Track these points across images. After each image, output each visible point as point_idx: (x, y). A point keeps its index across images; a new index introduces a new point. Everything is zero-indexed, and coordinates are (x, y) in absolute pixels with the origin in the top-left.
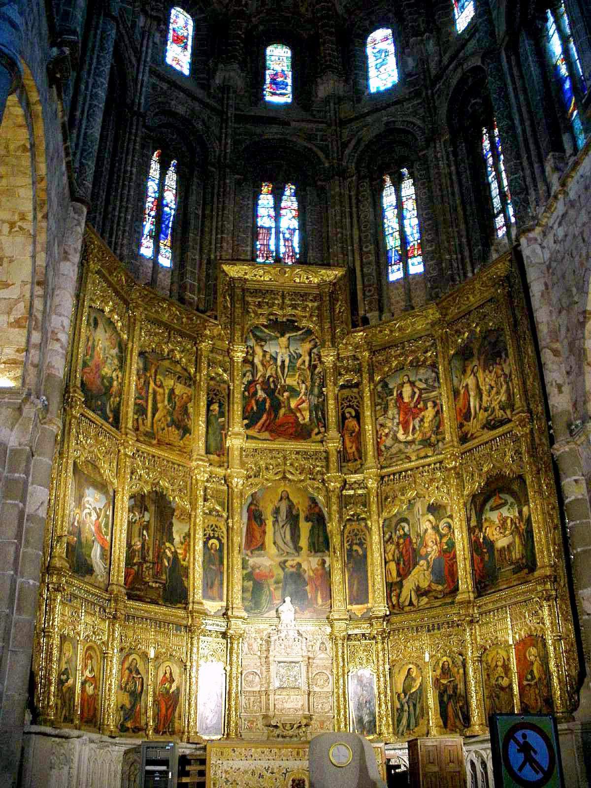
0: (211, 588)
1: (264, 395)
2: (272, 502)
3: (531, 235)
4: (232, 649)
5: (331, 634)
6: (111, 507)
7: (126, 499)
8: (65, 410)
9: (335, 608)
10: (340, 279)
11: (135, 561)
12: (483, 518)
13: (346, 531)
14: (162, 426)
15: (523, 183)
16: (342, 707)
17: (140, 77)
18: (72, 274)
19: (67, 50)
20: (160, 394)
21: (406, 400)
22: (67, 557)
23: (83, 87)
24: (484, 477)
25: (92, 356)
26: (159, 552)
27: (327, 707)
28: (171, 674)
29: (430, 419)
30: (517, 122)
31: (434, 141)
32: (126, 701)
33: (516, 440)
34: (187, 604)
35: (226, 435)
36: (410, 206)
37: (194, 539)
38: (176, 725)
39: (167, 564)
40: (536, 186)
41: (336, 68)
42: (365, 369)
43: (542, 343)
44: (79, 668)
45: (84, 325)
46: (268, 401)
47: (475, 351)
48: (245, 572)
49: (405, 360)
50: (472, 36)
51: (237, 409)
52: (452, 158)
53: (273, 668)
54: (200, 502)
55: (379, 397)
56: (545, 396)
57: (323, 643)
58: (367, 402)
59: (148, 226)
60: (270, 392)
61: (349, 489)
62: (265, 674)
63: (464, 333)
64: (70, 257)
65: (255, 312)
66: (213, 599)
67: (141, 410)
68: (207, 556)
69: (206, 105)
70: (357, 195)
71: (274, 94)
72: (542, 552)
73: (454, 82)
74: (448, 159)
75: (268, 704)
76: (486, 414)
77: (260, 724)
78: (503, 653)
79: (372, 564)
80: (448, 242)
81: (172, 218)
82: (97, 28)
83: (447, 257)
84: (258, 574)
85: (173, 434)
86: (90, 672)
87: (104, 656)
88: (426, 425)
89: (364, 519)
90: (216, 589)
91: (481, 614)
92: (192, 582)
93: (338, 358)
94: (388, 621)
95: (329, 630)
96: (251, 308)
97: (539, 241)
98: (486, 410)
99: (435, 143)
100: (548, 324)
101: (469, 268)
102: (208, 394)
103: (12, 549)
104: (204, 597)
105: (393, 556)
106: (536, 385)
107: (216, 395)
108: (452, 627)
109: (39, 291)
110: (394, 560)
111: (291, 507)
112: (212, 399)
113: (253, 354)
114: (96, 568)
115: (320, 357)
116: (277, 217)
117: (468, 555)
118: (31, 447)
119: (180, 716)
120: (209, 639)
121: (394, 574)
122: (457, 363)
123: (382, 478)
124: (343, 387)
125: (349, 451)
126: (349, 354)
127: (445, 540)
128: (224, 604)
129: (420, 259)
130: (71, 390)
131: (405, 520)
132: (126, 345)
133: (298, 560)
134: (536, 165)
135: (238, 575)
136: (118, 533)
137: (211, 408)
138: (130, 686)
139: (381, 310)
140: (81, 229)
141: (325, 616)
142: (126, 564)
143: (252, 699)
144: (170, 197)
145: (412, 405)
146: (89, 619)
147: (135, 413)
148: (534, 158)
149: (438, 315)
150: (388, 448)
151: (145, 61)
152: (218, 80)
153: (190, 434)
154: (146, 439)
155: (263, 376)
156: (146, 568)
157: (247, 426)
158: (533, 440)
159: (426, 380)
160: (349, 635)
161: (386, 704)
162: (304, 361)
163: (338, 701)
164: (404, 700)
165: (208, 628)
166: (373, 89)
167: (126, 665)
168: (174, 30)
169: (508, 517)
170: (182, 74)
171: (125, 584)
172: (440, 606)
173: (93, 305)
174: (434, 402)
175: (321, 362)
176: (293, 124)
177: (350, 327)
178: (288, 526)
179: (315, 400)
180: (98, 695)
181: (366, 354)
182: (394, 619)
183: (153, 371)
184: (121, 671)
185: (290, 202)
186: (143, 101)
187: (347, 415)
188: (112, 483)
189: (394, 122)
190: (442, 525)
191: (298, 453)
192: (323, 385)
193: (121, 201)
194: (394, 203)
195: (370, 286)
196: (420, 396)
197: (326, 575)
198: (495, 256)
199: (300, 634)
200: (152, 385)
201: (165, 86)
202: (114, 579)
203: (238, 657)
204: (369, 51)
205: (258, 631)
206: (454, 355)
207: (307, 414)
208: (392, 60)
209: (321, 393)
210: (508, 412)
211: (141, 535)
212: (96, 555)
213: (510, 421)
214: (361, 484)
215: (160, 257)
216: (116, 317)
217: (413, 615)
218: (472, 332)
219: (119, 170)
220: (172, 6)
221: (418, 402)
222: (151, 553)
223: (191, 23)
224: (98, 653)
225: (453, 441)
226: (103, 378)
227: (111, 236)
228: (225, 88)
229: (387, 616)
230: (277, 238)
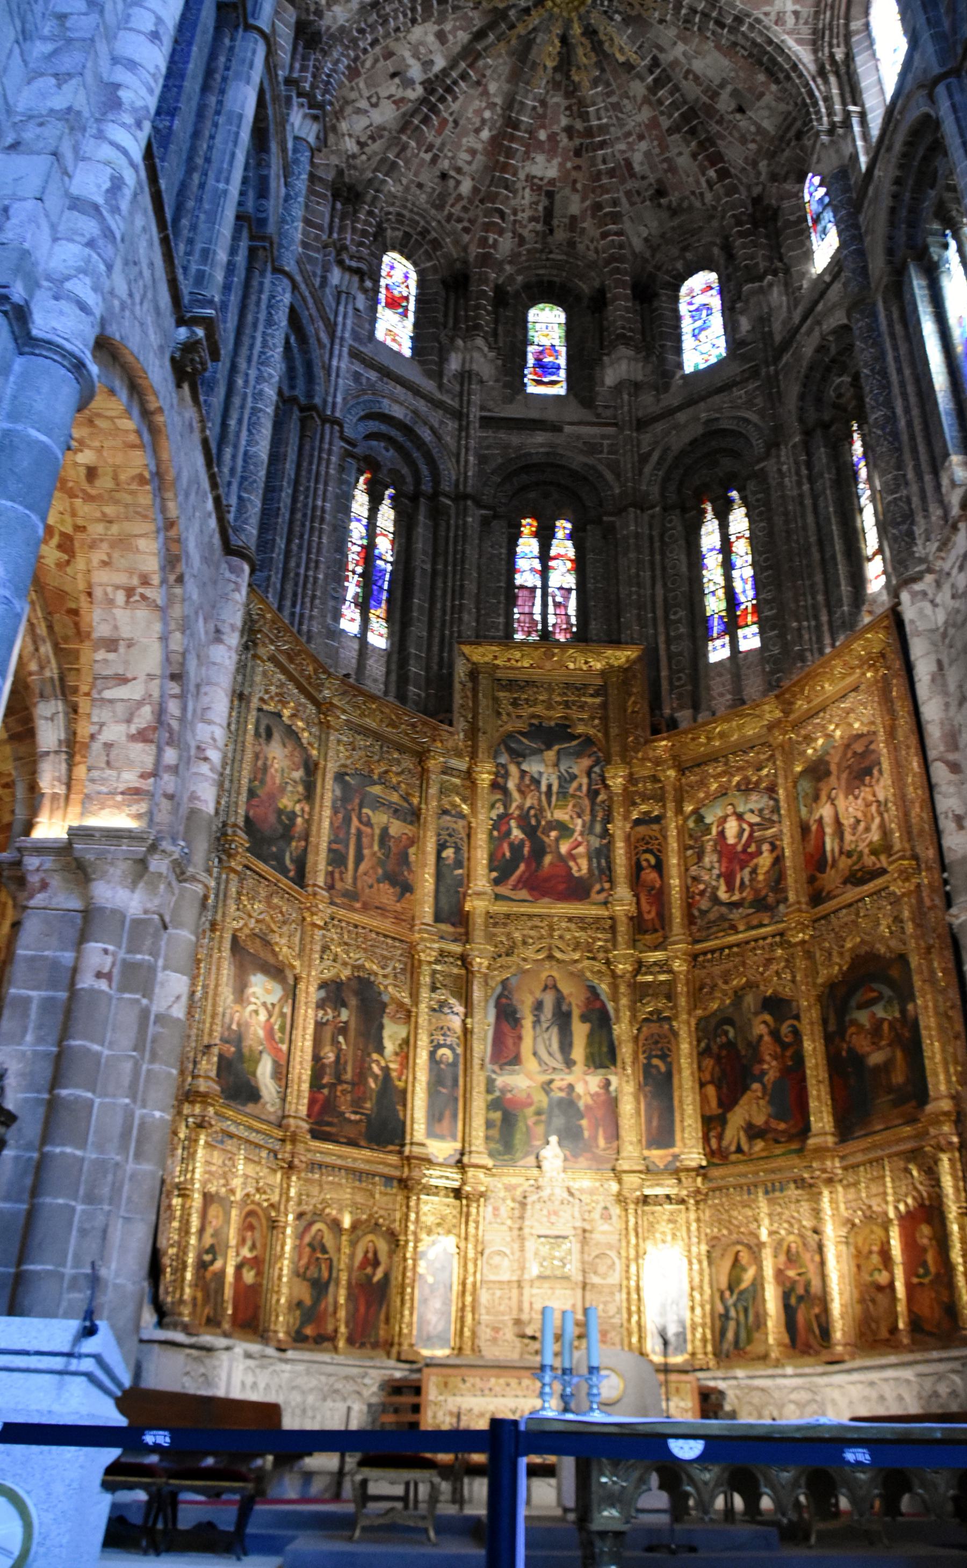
0: (440, 1120)
1: (522, 836)
2: (531, 993)
3: (917, 587)
4: (468, 1215)
5: (619, 1194)
7: (312, 989)
8: (220, 861)
9: (624, 1154)
10: (635, 662)
12: (847, 1018)
13: (642, 1037)
15: (905, 507)
16: (634, 1308)
17: (335, 363)
18: (227, 662)
19: (200, 332)
21: (731, 840)
22: (218, 1075)
23: (240, 382)
24: (847, 957)
25: (263, 782)
26: (362, 1068)
27: (612, 1309)
28: (375, 1253)
29: (765, 869)
30: (899, 410)
31: (777, 445)
32: (304, 1293)
33: (896, 901)
34: (403, 1145)
35: (465, 895)
36: (741, 549)
37: (415, 1047)
38: (382, 1333)
39: (373, 1085)
40: (925, 510)
41: (631, 338)
42: (670, 795)
43: (932, 754)
44: (233, 1242)
45: (250, 737)
46: (527, 844)
47: (833, 768)
48: (490, 1097)
49: (730, 781)
50: (835, 277)
51: (481, 856)
52: (804, 472)
53: (530, 1245)
54: (425, 994)
55: (691, 836)
56: (938, 833)
57: (606, 1208)
58: (673, 845)
59: (352, 588)
60: (531, 831)
61: (646, 974)
62: (518, 1254)
63: (816, 739)
64: (225, 637)
65: (508, 714)
66: (441, 1137)
67: (337, 859)
69: (437, 404)
70: (662, 536)
71: (539, 383)
72: (936, 1075)
73: (808, 351)
74: (798, 473)
75: (520, 1302)
76: (850, 862)
77: (509, 1333)
78: (879, 1232)
79: (681, 1087)
80: (797, 601)
81: (387, 577)
82: (261, 291)
83: (795, 624)
84: (510, 1100)
85: (386, 894)
87: (273, 1225)
88: (761, 878)
89: (668, 1019)
90: (446, 1122)
91: (845, 1169)
92: (409, 1112)
93: (631, 779)
94: (705, 1177)
95: (614, 1187)
96: (506, 706)
97: (930, 596)
98: (849, 855)
99: (779, 449)
100: (942, 723)
101: (827, 641)
102: (439, 835)
103: (128, 1066)
104: (430, 1134)
105: (712, 1074)
106: (924, 815)
108: (803, 1188)
109: (175, 689)
110: (711, 1082)
111: (560, 1000)
113: (506, 775)
115: (603, 780)
116: (544, 573)
117: (823, 1075)
118: (162, 917)
119: (387, 1321)
120: (435, 1199)
121: (714, 1103)
122: (805, 786)
123: (695, 957)
124: (637, 822)
125: (647, 917)
126: (646, 773)
127: (788, 1053)
128: (458, 1145)
129: (755, 629)
130: (230, 831)
131: (730, 1021)
132: (316, 765)
133: (570, 1079)
134: (928, 478)
135: (479, 1103)
136: (300, 1039)
137: (444, 854)
138: (313, 1272)
139: (696, 707)
140: (241, 596)
141: (609, 1166)
142: (312, 1086)
143: (498, 1293)
144: (384, 545)
145: (739, 848)
146: (251, 1170)
147: (329, 864)
148: (925, 467)
149: (778, 714)
150: (704, 913)
151: (342, 339)
152: (454, 364)
154: (345, 900)
155: (520, 807)
157: (497, 882)
158: (920, 901)
159: (761, 811)
160: (646, 1196)
161: (702, 1306)
162: (580, 786)
163: (628, 1300)
164: (730, 1302)
165: (433, 1182)
166: (688, 368)
167: (307, 1239)
168: (387, 286)
169: (883, 1020)
170: (398, 354)
171: (309, 1116)
172: (783, 1154)
173: (265, 707)
174: (772, 844)
175: (607, 787)
176: (568, 429)
177: (648, 732)
178: (555, 1031)
179: (596, 842)
180: (260, 1285)
181: (672, 773)
182: (715, 1172)
183: (357, 801)
184: (297, 1248)
185: (563, 547)
186: (339, 399)
187: (644, 864)
188: (293, 967)
189: (717, 419)
190: (785, 1029)
191: (570, 919)
192: (608, 819)
193: (309, 552)
194: (718, 546)
195: (679, 671)
196: (751, 835)
197: (612, 1104)
198: (867, 619)
199: (571, 1194)
200: (355, 822)
201: (373, 375)
202: (291, 1109)
203: (477, 1228)
204: (683, 308)
205: (509, 1188)
206: (802, 773)
207: (584, 863)
208: (717, 322)
209: (605, 833)
210: (883, 858)
211: (335, 1042)
213: (883, 872)
214: (664, 966)
215: (370, 634)
216: (300, 724)
217: (742, 1168)
218: (829, 736)
219: (305, 505)
220: (385, 251)
221: (747, 845)
222: (349, 1069)
223: (413, 276)
224: (264, 1221)
225: (799, 902)
226: (280, 812)
227: (294, 605)
228: (465, 376)
229: (702, 1167)
230: (545, 605)
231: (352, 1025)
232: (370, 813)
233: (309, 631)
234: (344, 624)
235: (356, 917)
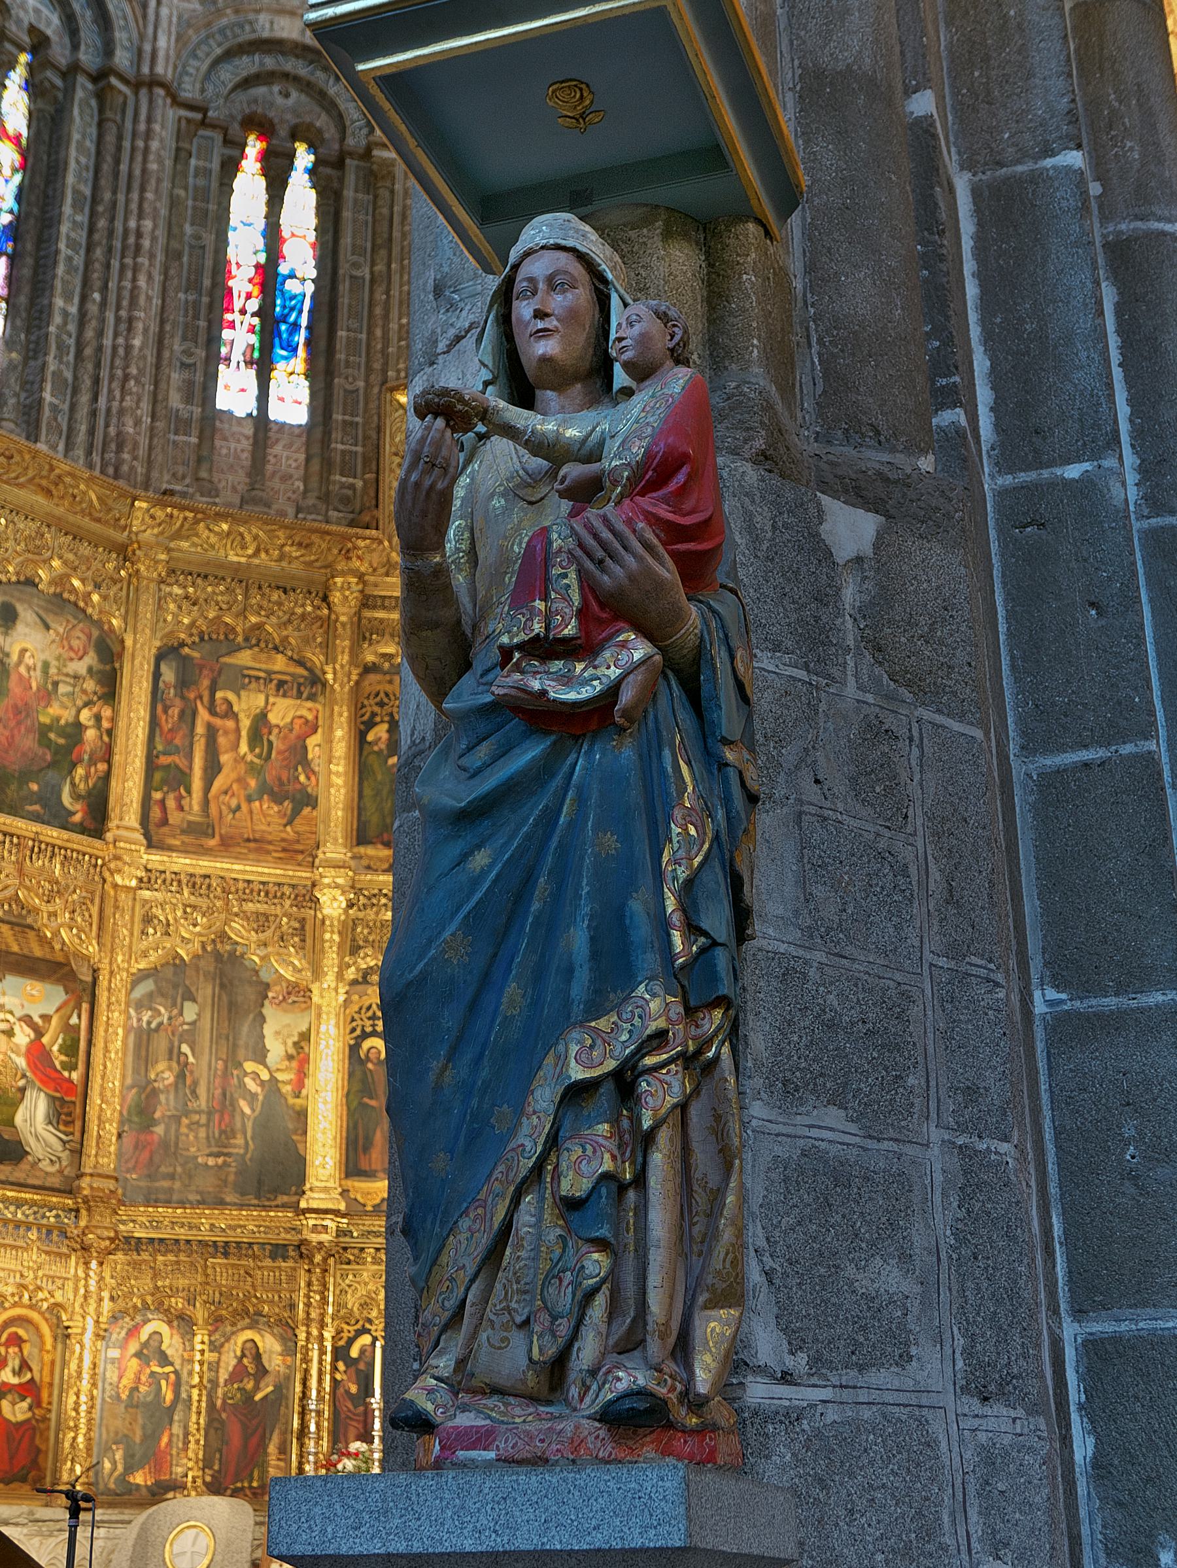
6: (85, 1006)
11: (157, 1115)
14: (234, 803)
20: (226, 733)
28: (258, 1357)
39: (247, 1110)
54: (331, 958)
68: (358, 1073)
86: (17, 1373)
107: (381, 704)
112: (374, 715)
114: (32, 1145)
132: (122, 641)
137: (370, 737)
153: (314, 808)
156: (188, 1127)
183: (206, 683)
200: (203, 715)
211: (173, 1054)
212: (32, 1118)
222: (202, 1091)
231: (206, 1023)
232: (231, 696)
233: (119, 434)
234: (223, 401)
235: (205, 865)
